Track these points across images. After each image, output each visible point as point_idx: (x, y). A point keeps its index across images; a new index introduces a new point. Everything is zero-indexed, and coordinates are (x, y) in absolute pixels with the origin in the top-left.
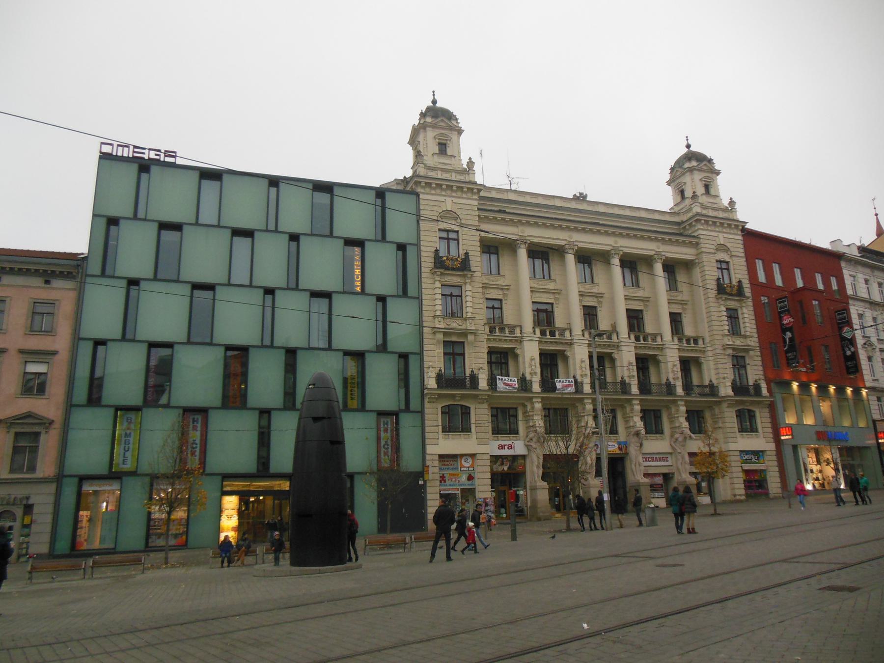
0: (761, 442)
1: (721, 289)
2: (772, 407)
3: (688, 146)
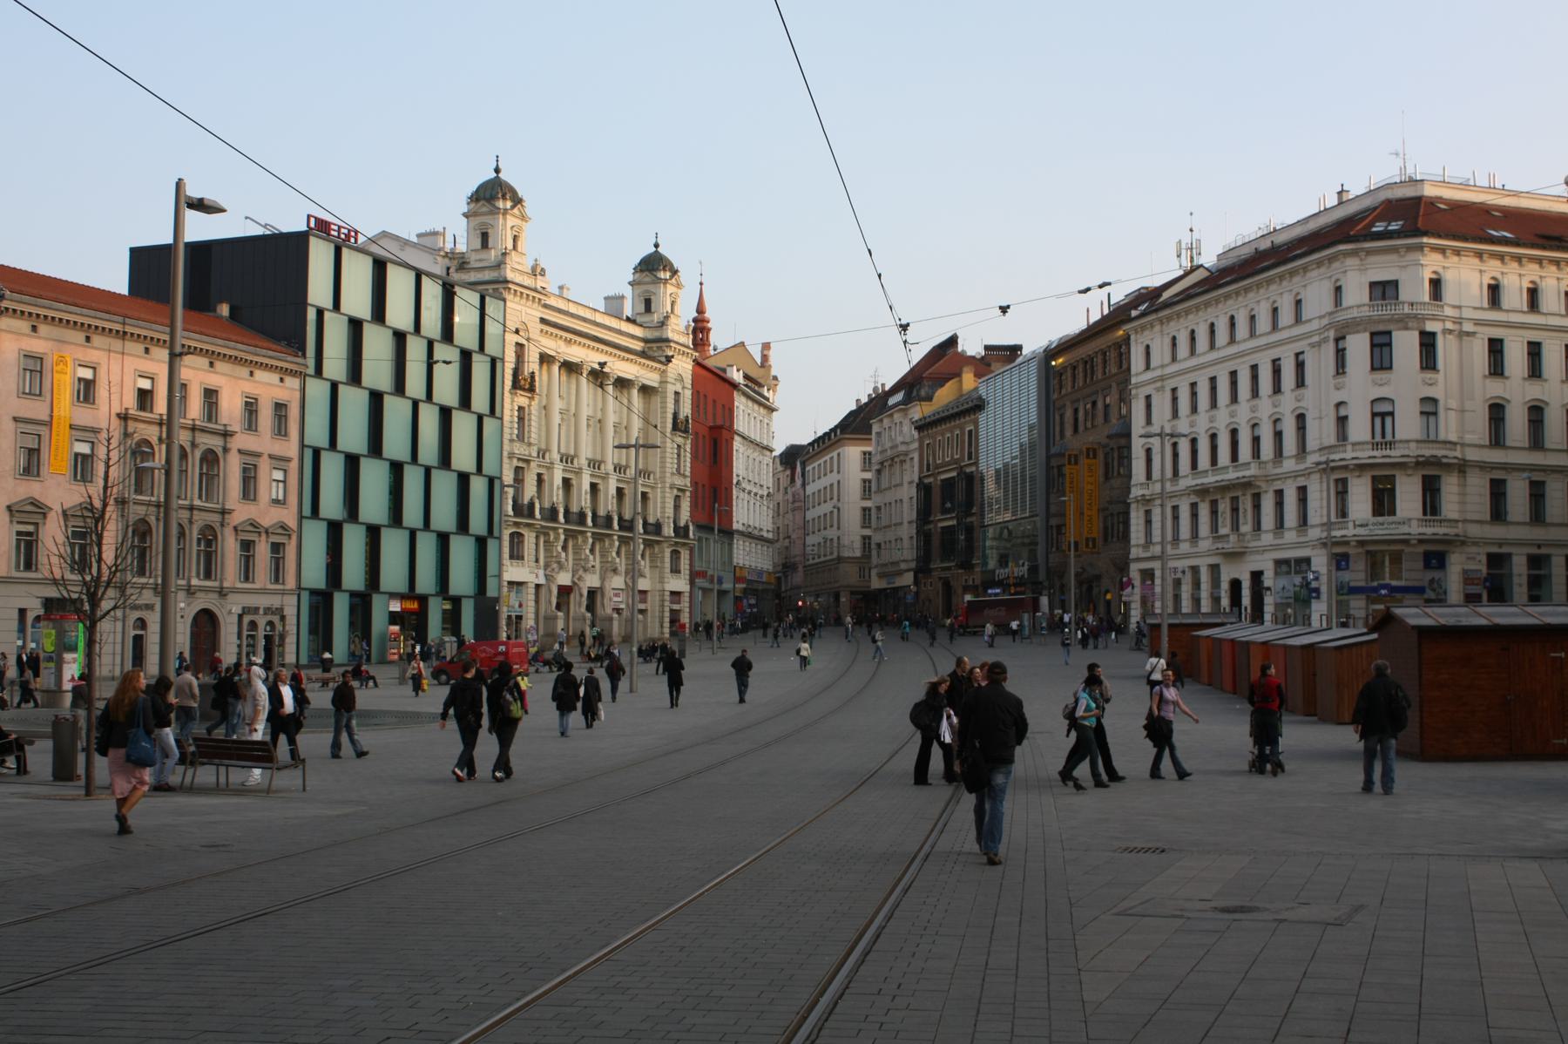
0: (680, 584)
1: (675, 427)
2: (691, 551)
3: (656, 246)
